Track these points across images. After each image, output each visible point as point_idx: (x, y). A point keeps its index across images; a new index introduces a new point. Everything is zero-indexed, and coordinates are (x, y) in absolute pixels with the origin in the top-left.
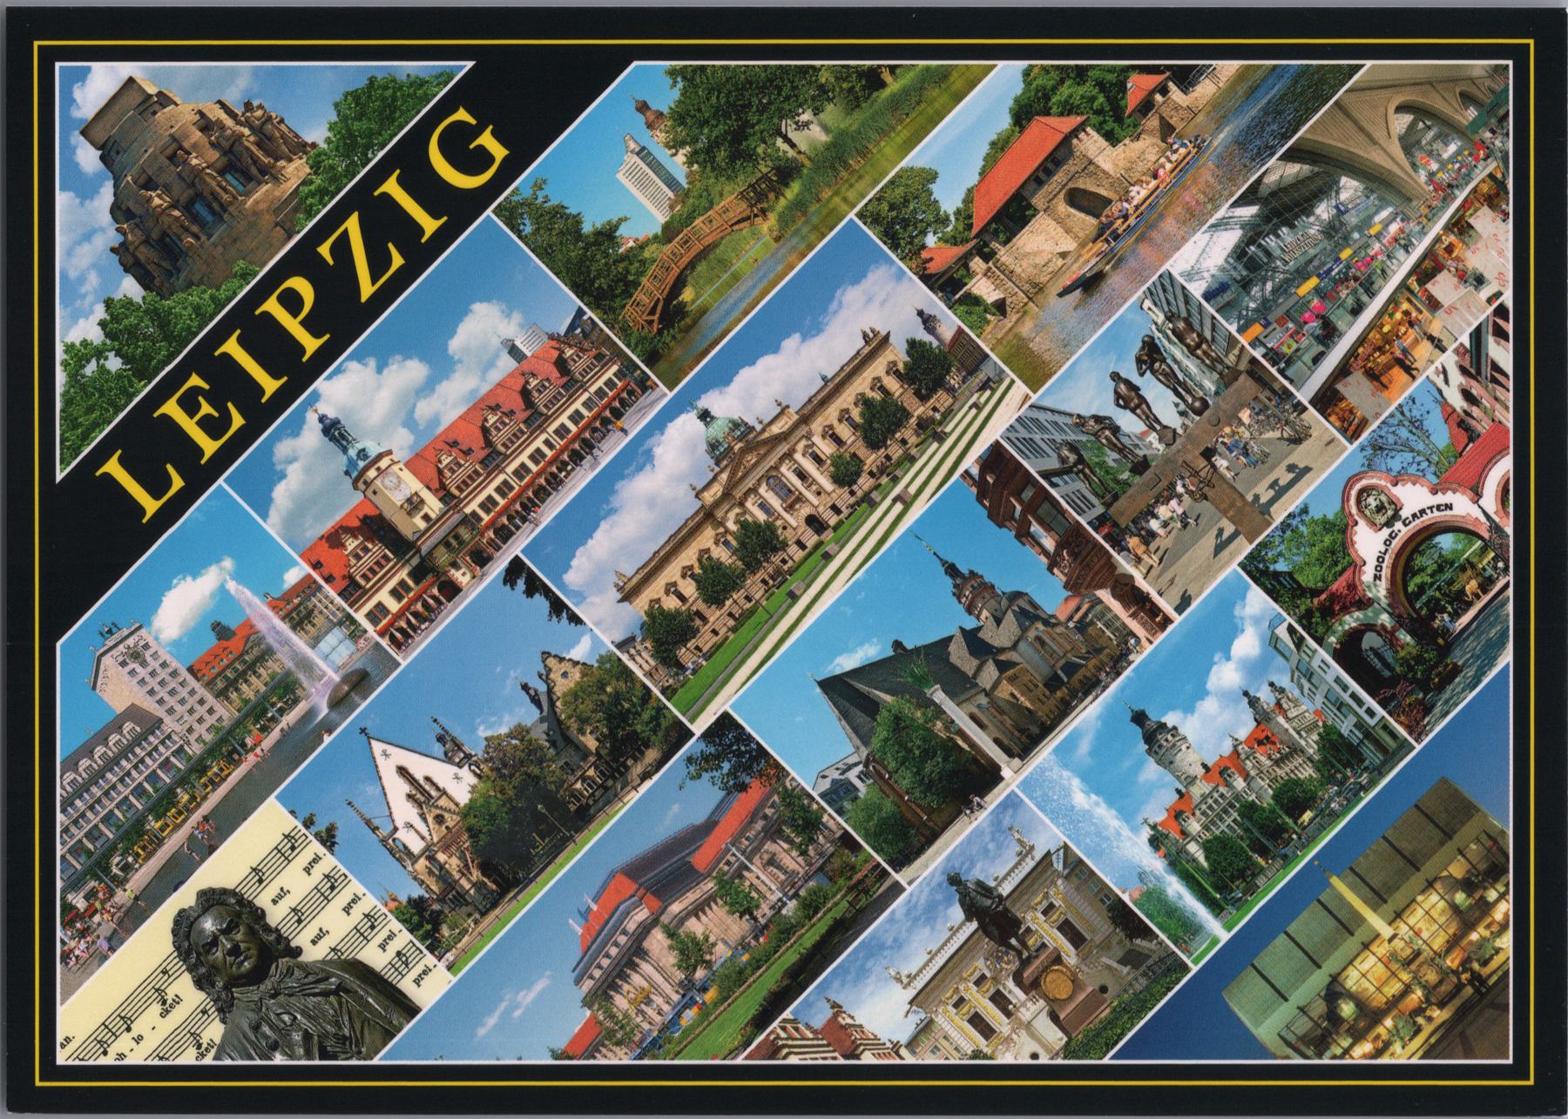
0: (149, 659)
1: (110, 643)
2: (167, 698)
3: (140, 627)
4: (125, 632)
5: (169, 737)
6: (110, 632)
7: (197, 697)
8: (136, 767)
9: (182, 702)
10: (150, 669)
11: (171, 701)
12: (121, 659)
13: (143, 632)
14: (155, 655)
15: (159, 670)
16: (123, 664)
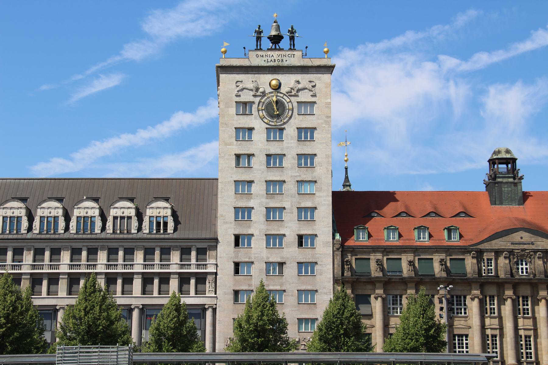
0: (290, 131)
1: (255, 60)
2: (258, 215)
3: (329, 69)
4: (295, 59)
5: (201, 279)
6: (276, 40)
7: (304, 255)
8: (147, 279)
9: (274, 240)
10: (274, 149)
11: (258, 226)
12: (247, 97)
13: (322, 80)
14: (306, 133)
15: (289, 162)
16: (244, 107)
